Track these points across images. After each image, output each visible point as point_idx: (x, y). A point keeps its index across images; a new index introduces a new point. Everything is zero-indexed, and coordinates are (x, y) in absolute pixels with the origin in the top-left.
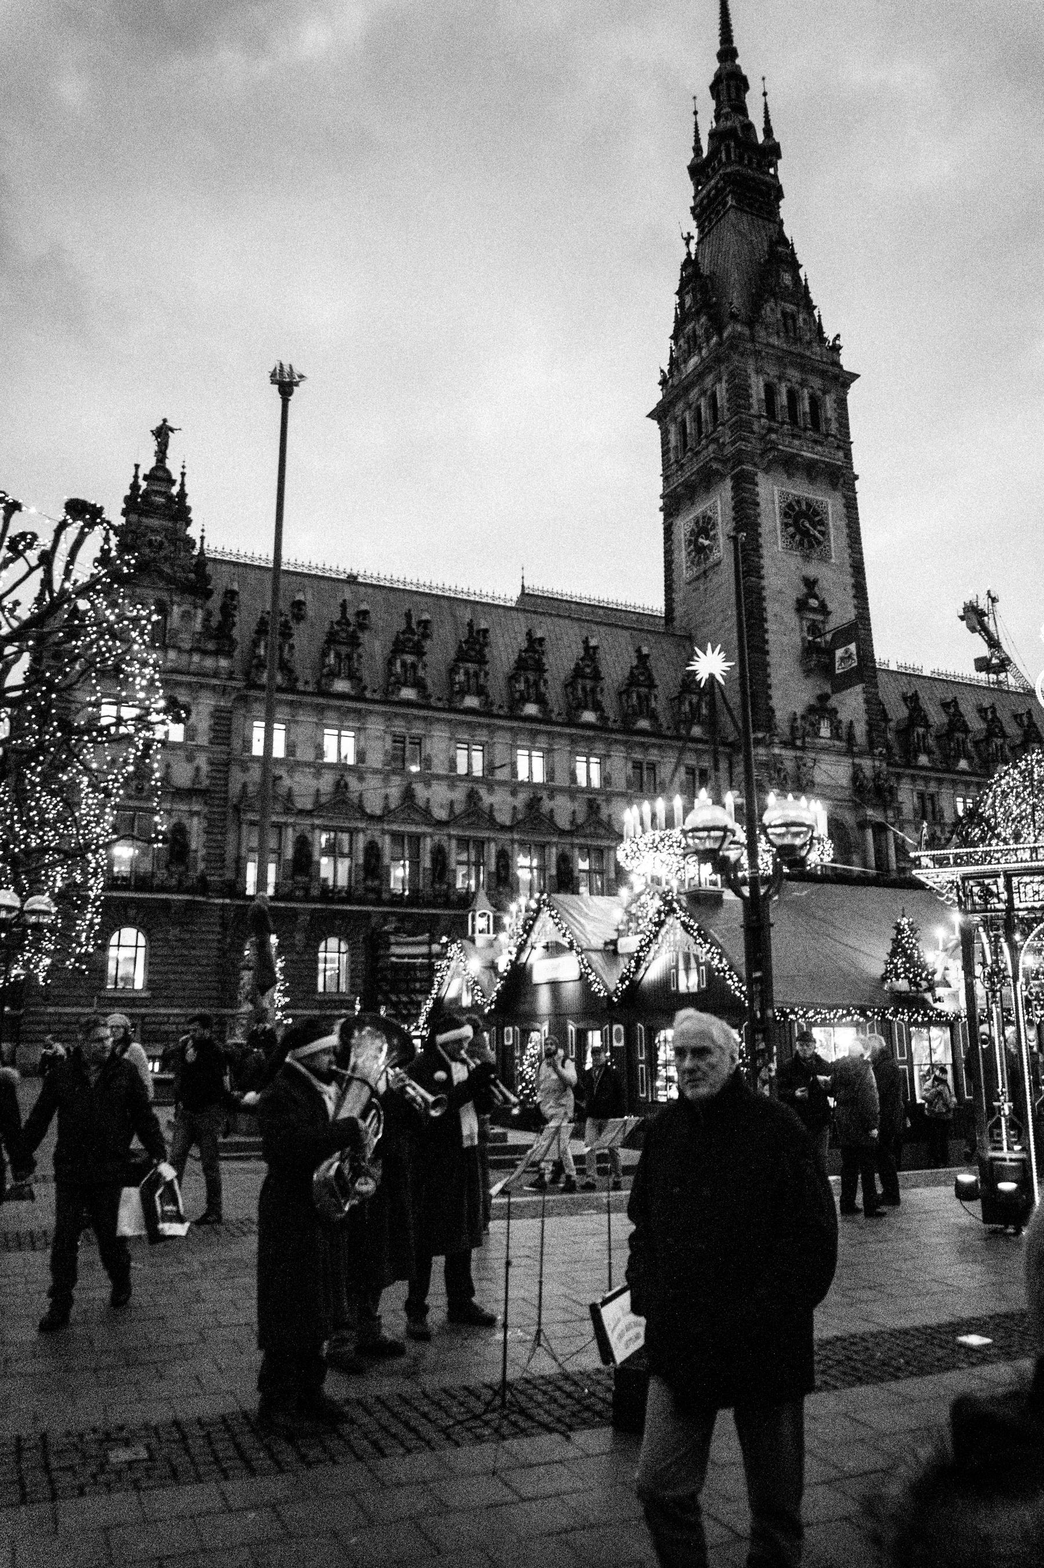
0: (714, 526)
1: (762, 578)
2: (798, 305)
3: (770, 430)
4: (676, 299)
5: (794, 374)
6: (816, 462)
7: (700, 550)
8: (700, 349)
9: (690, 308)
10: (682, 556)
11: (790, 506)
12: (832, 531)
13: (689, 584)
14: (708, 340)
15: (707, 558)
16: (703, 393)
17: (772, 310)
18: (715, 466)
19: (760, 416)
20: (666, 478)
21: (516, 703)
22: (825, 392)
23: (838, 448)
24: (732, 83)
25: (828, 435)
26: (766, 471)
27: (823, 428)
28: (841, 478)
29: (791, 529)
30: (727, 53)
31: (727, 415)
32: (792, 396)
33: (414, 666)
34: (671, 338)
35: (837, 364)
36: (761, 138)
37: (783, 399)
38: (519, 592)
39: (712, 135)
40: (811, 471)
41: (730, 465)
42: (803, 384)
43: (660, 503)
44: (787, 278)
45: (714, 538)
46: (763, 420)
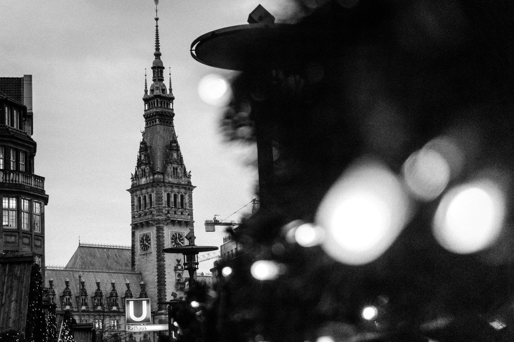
0: (150, 240)
1: (164, 261)
3: (168, 212)
5: (176, 190)
6: (182, 221)
7: (145, 246)
10: (138, 244)
11: (173, 236)
15: (147, 249)
18: (151, 222)
20: (133, 217)
21: (95, 307)
22: (185, 194)
23: (189, 215)
24: (159, 70)
25: (186, 209)
29: (174, 244)
30: (158, 55)
33: (69, 299)
35: (190, 182)
36: (168, 92)
37: (172, 199)
38: (78, 245)
39: (152, 91)
40: (180, 223)
41: (156, 222)
42: (178, 193)
44: (175, 155)
45: (150, 244)
46: (166, 208)
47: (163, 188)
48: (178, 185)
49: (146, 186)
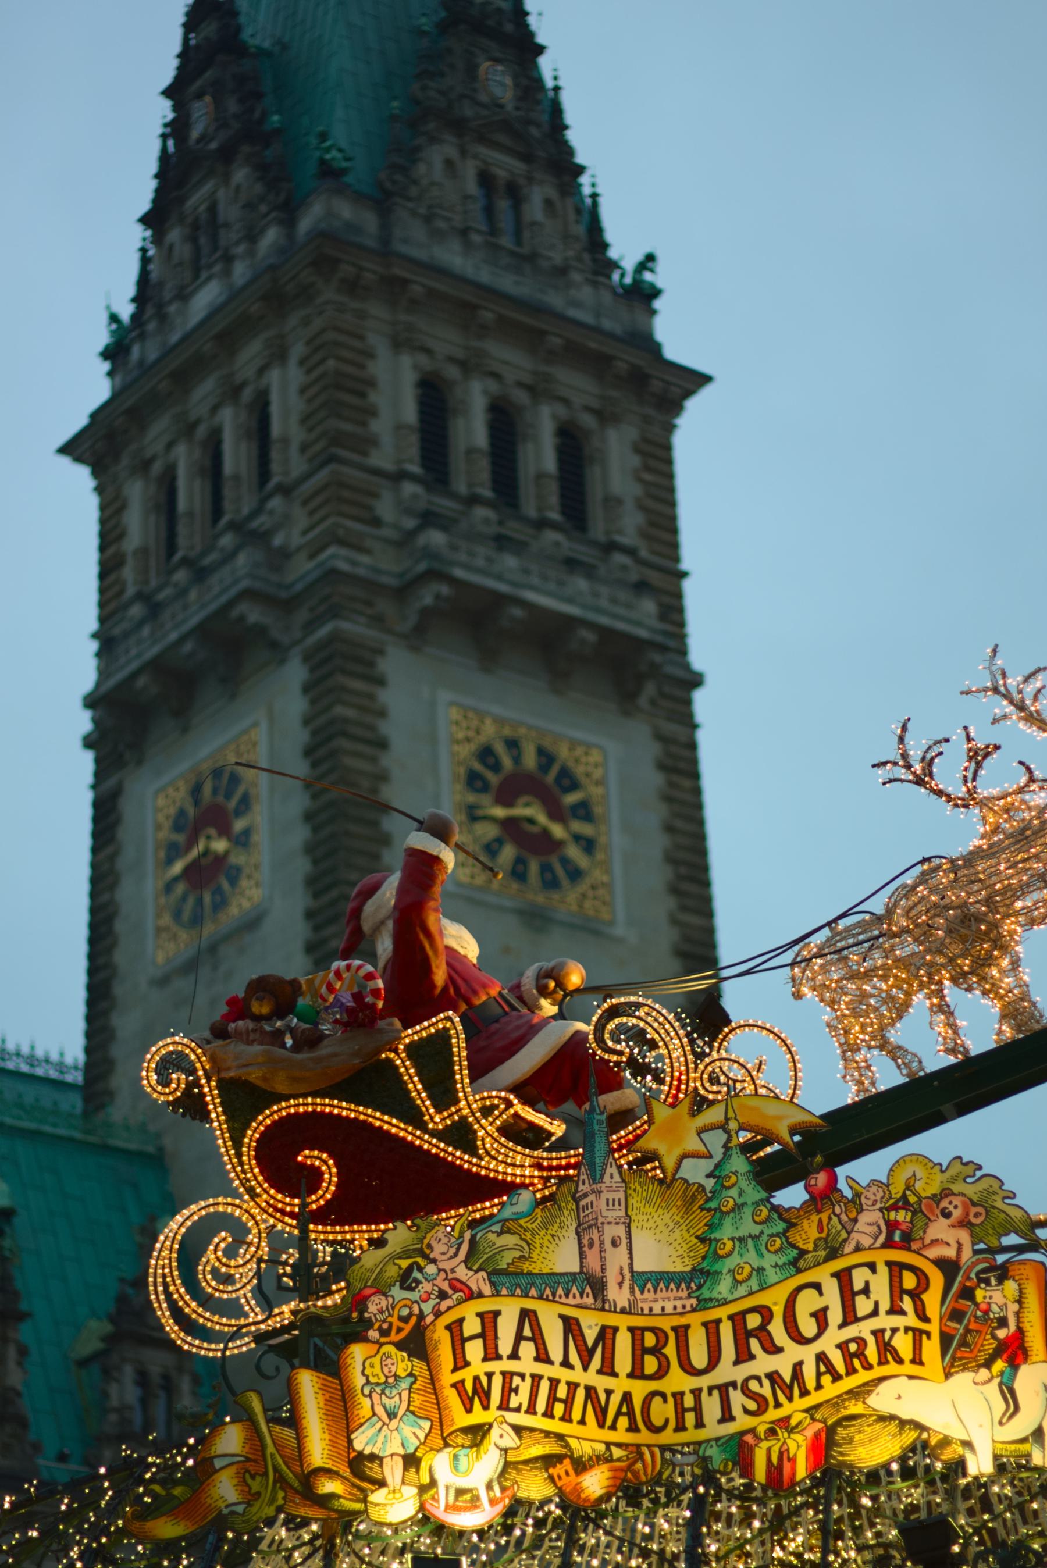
0: (245, 804)
2: (527, 158)
3: (429, 519)
4: (165, 110)
5: (511, 360)
8: (228, 259)
9: (203, 138)
10: (145, 890)
11: (486, 754)
12: (615, 838)
13: (163, 981)
14: (252, 237)
15: (221, 903)
16: (233, 392)
17: (449, 163)
18: (254, 614)
19: (400, 476)
22: (606, 417)
23: (641, 587)
25: (611, 547)
26: (417, 637)
27: (598, 530)
28: (647, 674)
31: (298, 465)
32: (504, 423)
34: (145, 220)
37: (473, 430)
40: (551, 649)
41: (302, 615)
42: (538, 390)
43: (84, 722)
44: (498, 81)
45: (243, 840)
46: (409, 488)
47: (377, 310)
48: (529, 326)
49: (227, 332)
